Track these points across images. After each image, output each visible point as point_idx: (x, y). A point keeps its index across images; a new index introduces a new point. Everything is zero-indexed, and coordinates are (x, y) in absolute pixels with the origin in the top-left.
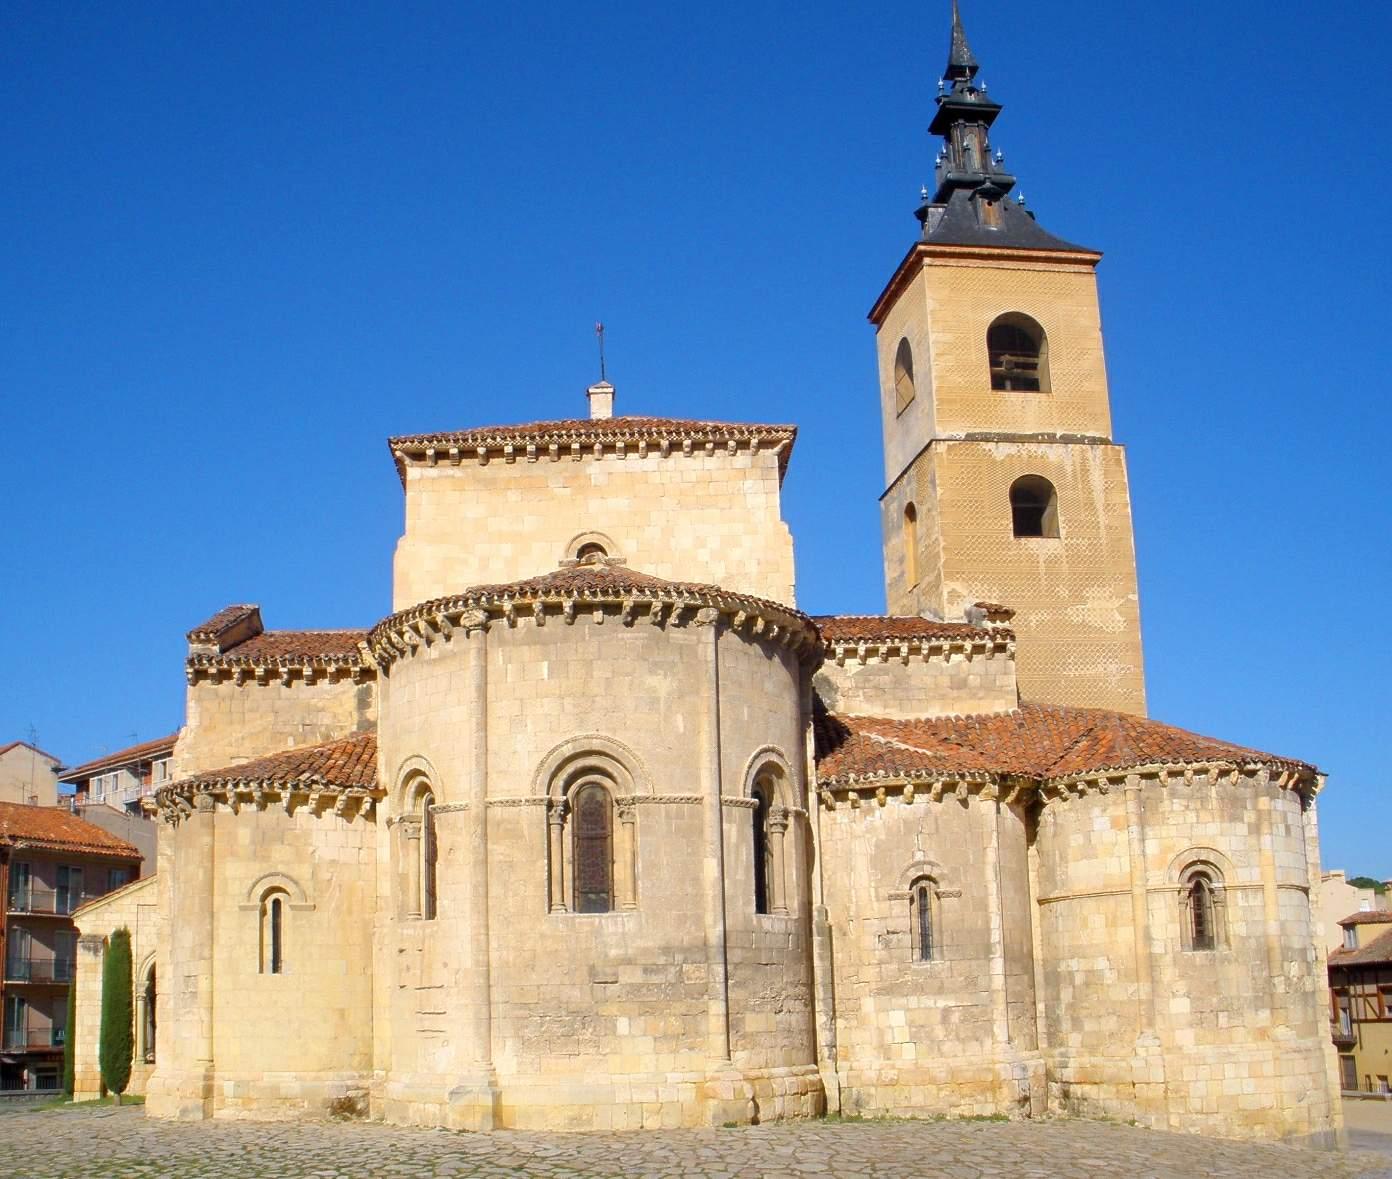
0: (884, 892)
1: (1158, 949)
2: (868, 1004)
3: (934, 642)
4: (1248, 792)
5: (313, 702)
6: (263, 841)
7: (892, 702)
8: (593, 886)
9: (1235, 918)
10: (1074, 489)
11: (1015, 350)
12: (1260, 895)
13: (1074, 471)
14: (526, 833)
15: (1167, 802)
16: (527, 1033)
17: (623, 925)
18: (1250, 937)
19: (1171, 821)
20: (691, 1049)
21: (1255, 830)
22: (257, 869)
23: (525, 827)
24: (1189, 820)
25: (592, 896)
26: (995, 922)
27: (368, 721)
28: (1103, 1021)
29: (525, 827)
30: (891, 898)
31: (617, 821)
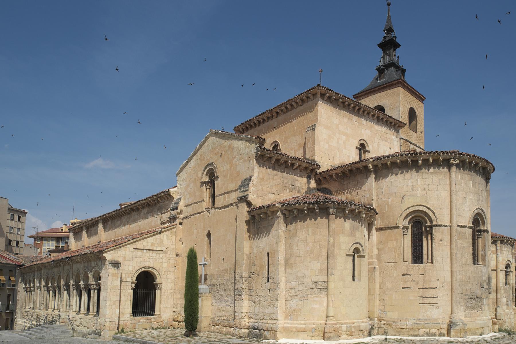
6: (353, 230)
22: (352, 240)
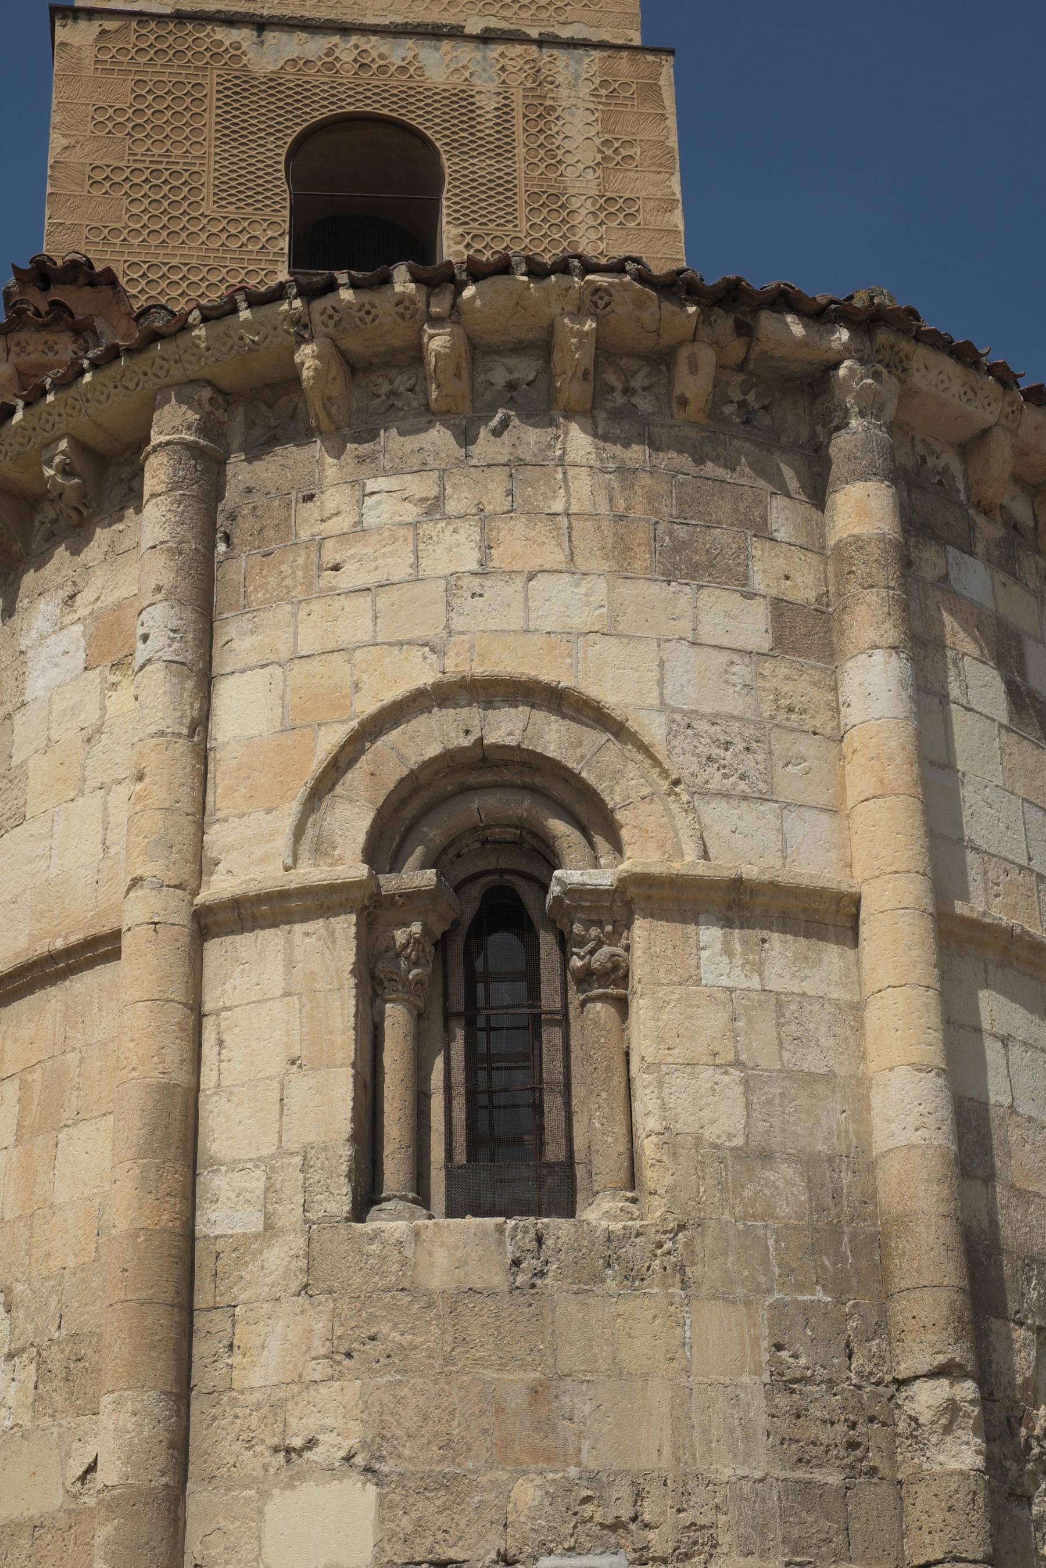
9: (678, 1050)
10: (503, 149)
12: (832, 956)
13: (505, 110)
15: (334, 498)
18: (766, 1156)
19: (351, 577)
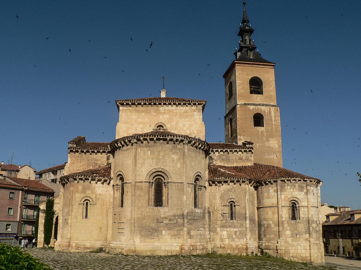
0: (223, 204)
1: (284, 219)
2: (218, 229)
3: (235, 149)
4: (305, 185)
5: (97, 158)
7: (225, 162)
8: (158, 202)
10: (268, 116)
11: (256, 86)
14: (144, 189)
15: (286, 187)
16: (142, 233)
17: (165, 210)
20: (179, 238)
21: (307, 193)
22: (83, 195)
23: (144, 187)
24: (291, 191)
25: (158, 203)
26: (247, 212)
27: (109, 163)
28: (271, 235)
29: (144, 187)
30: (224, 206)
31: (164, 187)
